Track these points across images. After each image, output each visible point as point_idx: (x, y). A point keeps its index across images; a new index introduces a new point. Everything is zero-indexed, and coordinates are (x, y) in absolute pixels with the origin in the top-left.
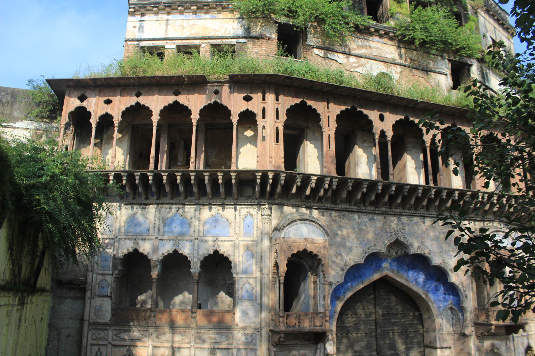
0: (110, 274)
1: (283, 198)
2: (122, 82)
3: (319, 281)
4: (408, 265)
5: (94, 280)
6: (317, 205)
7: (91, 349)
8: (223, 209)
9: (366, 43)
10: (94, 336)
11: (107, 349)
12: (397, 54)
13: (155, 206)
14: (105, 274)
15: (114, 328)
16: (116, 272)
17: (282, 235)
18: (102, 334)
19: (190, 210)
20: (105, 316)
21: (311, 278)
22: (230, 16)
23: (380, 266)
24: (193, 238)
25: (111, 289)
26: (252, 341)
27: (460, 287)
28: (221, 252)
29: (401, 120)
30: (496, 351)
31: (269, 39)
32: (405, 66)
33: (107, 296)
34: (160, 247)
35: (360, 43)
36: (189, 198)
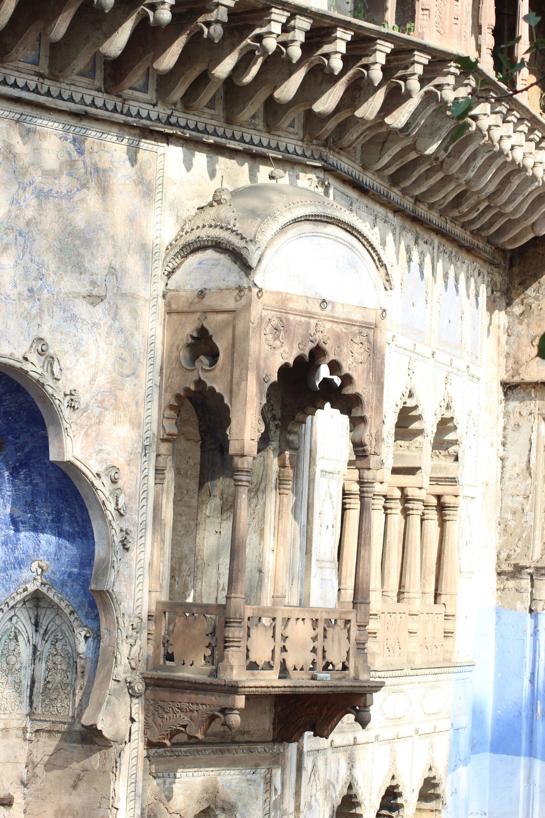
27: (104, 489)
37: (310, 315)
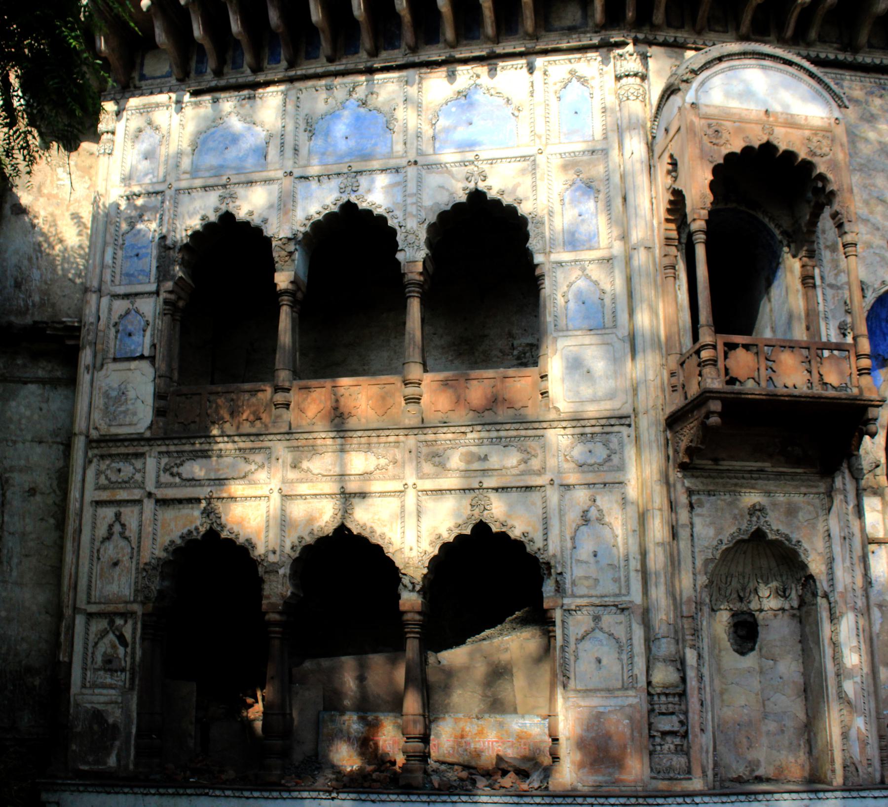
0: (150, 294)
1: (680, 27)
3: (822, 278)
5: (103, 315)
7: (95, 517)
8: (492, 72)
10: (103, 477)
11: (141, 513)
13: (282, 87)
14: (137, 295)
15: (164, 449)
16: (169, 285)
17: (690, 97)
18: (127, 469)
19: (388, 87)
20: (135, 414)
21: (792, 266)
24: (404, 162)
25: (152, 335)
26: (609, 458)
28: (492, 194)
33: (142, 357)
34: (299, 197)
36: (384, 55)
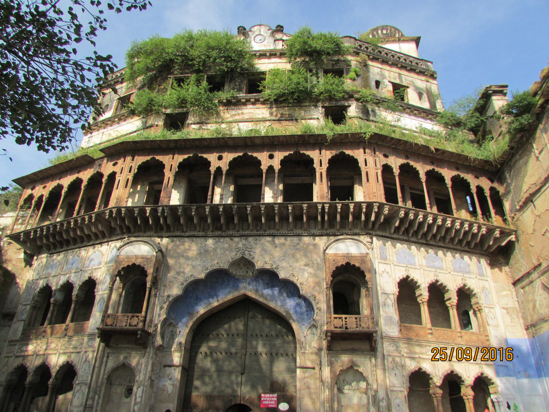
2: (51, 172)
4: (267, 284)
6: (167, 234)
9: (240, 112)
12: (268, 113)
22: (138, 118)
23: (238, 286)
29: (239, 157)
30: (355, 368)
31: (157, 126)
32: (274, 120)
35: (234, 112)
37: (345, 256)
